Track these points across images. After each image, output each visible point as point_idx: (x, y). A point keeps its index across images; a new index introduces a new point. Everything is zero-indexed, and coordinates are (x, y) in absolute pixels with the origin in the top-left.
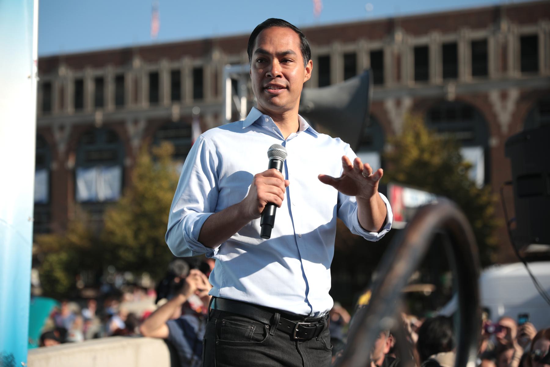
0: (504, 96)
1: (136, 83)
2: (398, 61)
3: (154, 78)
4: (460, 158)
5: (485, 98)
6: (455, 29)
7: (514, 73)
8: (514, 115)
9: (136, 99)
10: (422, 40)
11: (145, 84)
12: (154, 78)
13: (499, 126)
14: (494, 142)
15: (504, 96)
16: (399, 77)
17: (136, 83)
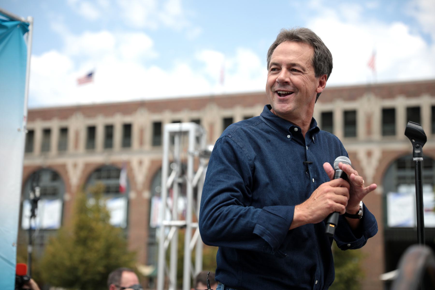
0: (369, 154)
1: (77, 134)
3: (92, 130)
6: (331, 100)
8: (377, 169)
9: (76, 146)
11: (83, 135)
12: (92, 130)
15: (369, 154)
17: (77, 134)
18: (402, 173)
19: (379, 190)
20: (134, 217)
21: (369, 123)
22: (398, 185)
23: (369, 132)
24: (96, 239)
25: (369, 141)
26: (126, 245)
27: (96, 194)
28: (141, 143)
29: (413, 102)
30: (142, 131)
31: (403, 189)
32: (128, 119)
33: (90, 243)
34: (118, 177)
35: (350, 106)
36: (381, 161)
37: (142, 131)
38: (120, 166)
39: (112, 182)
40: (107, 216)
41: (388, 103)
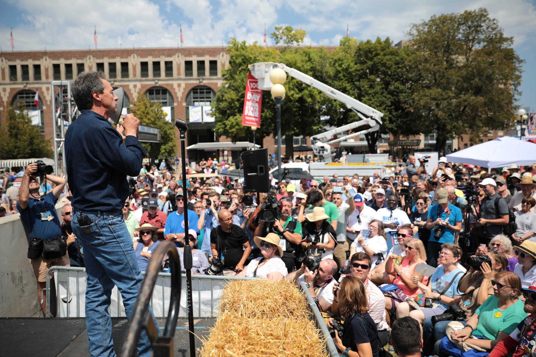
0: (179, 85)
2: (134, 67)
4: (162, 111)
5: (172, 85)
7: (183, 76)
8: (183, 93)
10: (145, 60)
13: (177, 98)
14: (175, 104)
15: (179, 85)
16: (135, 75)
18: (196, 95)
19: (184, 104)
20: (46, 120)
21: (179, 69)
22: (194, 101)
23: (179, 74)
24: (25, 134)
25: (179, 79)
26: (43, 137)
27: (21, 108)
28: (47, 77)
29: (201, 59)
30: (47, 70)
31: (196, 104)
32: (37, 63)
33: (19, 136)
34: (34, 97)
35: (169, 59)
36: (185, 89)
37: (47, 70)
38: (35, 90)
39: (30, 100)
40: (30, 121)
41: (188, 59)
